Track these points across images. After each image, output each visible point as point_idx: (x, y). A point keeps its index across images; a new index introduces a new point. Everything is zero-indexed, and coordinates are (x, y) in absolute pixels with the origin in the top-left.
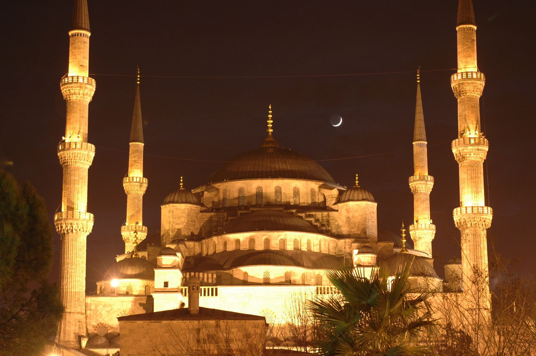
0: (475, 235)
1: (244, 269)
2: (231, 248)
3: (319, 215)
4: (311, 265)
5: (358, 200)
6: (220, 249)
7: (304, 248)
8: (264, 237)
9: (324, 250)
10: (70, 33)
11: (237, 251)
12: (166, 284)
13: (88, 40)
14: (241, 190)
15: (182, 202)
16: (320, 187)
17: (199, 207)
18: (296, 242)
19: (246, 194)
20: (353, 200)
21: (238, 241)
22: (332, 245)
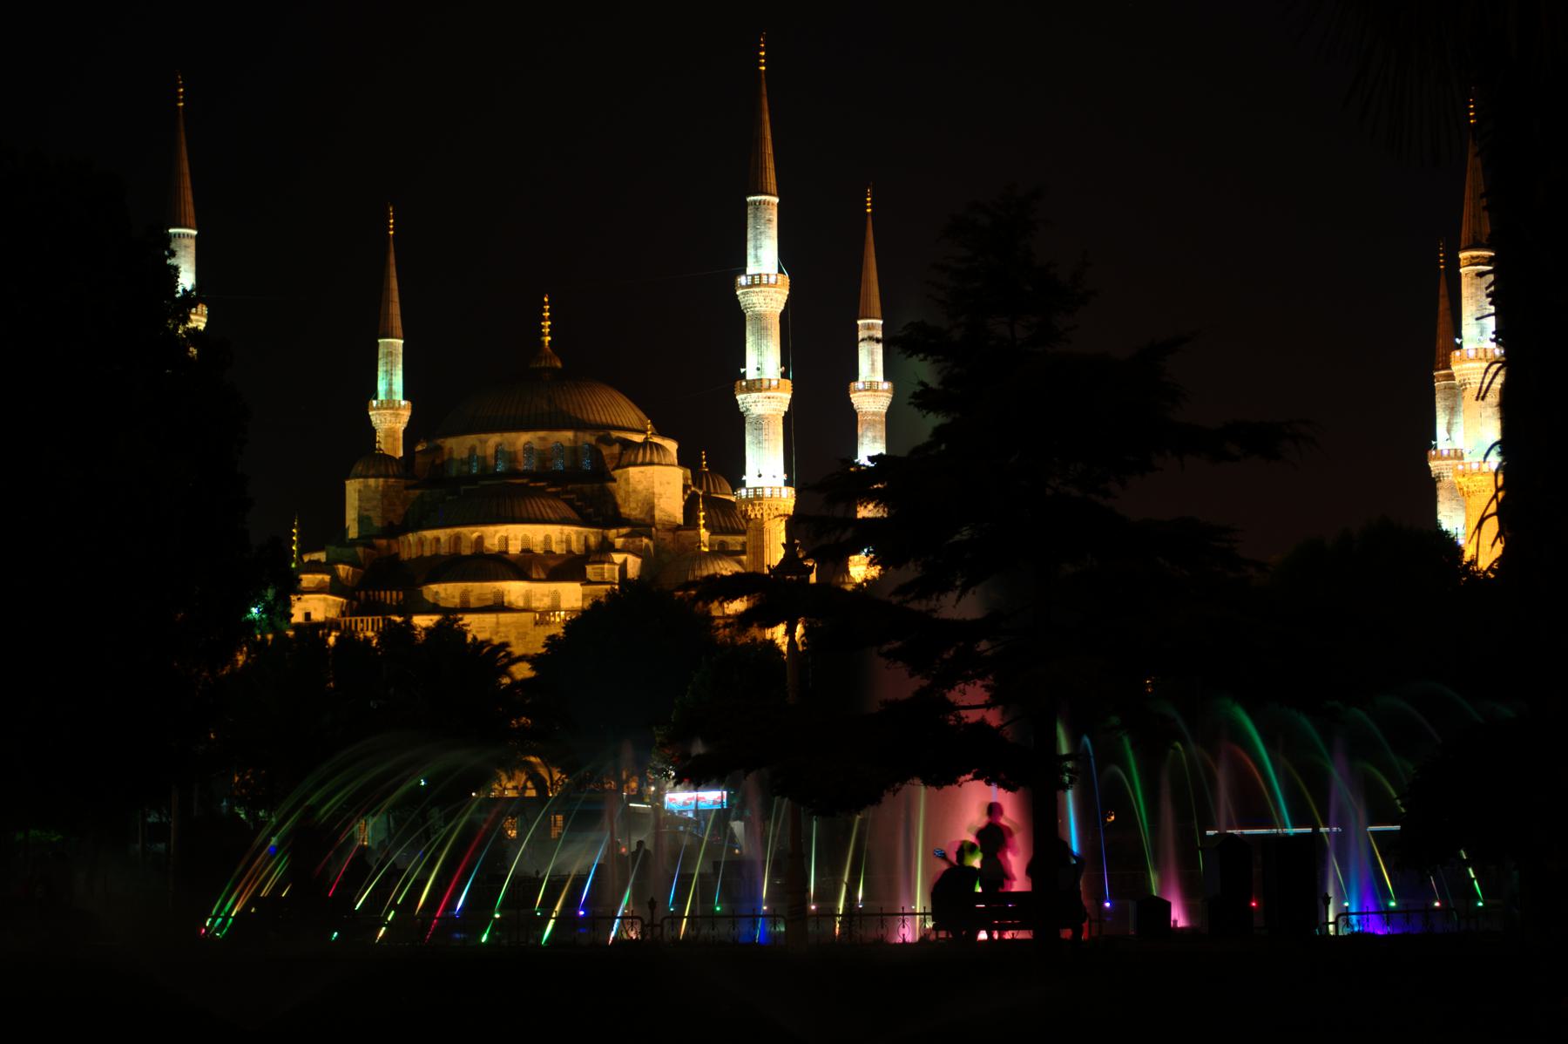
0: (760, 530)
1: (434, 587)
2: (427, 553)
3: (587, 488)
4: (543, 576)
5: (643, 464)
6: (414, 553)
7: (539, 550)
8: (475, 535)
11: (436, 556)
12: (308, 615)
13: (192, 243)
14: (473, 449)
16: (599, 440)
17: (403, 481)
18: (525, 540)
20: (635, 465)
21: (438, 540)
22: (592, 540)
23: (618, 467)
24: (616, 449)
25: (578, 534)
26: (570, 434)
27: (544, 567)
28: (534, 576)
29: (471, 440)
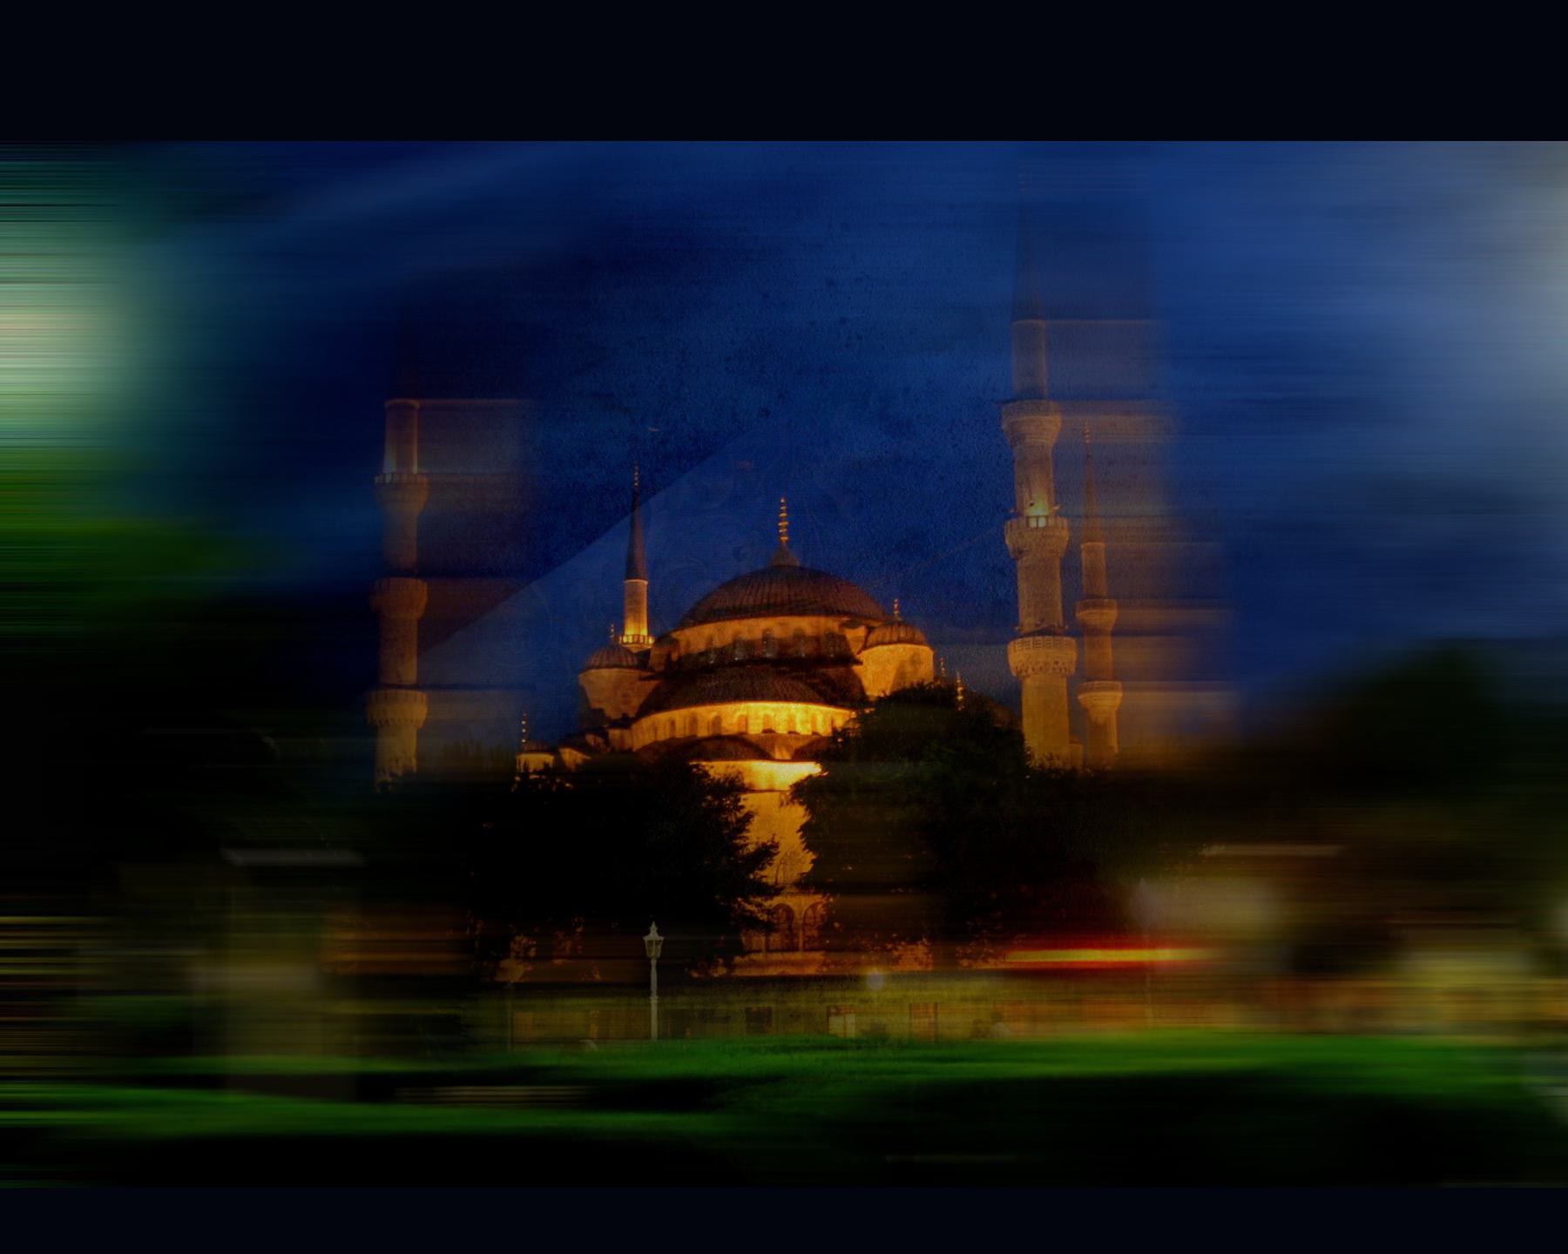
2: (663, 735)
3: (832, 672)
5: (890, 643)
7: (782, 730)
8: (714, 714)
9: (824, 729)
10: (387, 404)
11: (673, 738)
14: (710, 639)
15: (608, 667)
16: (843, 625)
17: (636, 673)
18: (767, 717)
19: (717, 643)
20: (883, 643)
23: (865, 647)
24: (861, 631)
25: (825, 714)
26: (813, 620)
27: (788, 748)
28: (777, 756)
29: (709, 629)
